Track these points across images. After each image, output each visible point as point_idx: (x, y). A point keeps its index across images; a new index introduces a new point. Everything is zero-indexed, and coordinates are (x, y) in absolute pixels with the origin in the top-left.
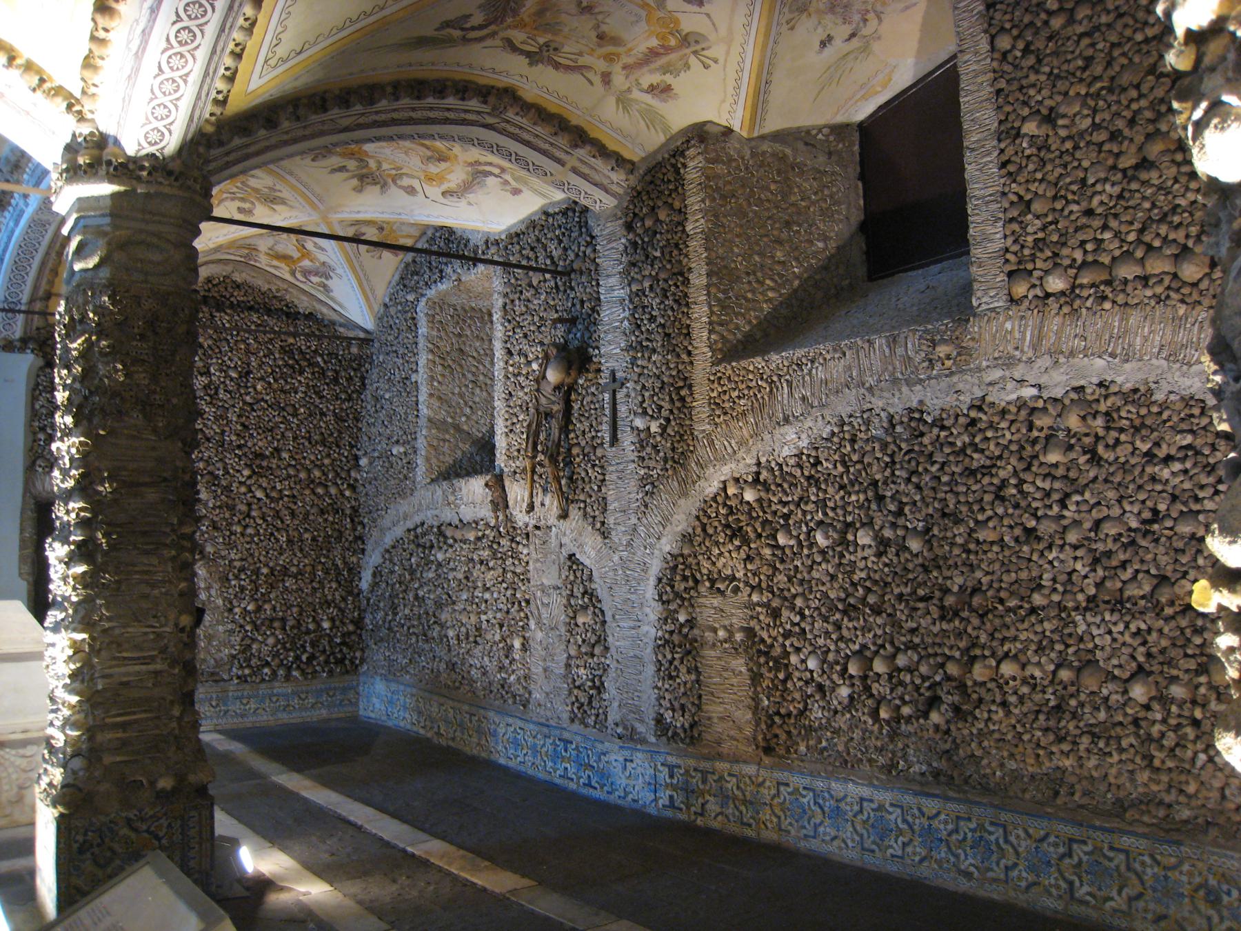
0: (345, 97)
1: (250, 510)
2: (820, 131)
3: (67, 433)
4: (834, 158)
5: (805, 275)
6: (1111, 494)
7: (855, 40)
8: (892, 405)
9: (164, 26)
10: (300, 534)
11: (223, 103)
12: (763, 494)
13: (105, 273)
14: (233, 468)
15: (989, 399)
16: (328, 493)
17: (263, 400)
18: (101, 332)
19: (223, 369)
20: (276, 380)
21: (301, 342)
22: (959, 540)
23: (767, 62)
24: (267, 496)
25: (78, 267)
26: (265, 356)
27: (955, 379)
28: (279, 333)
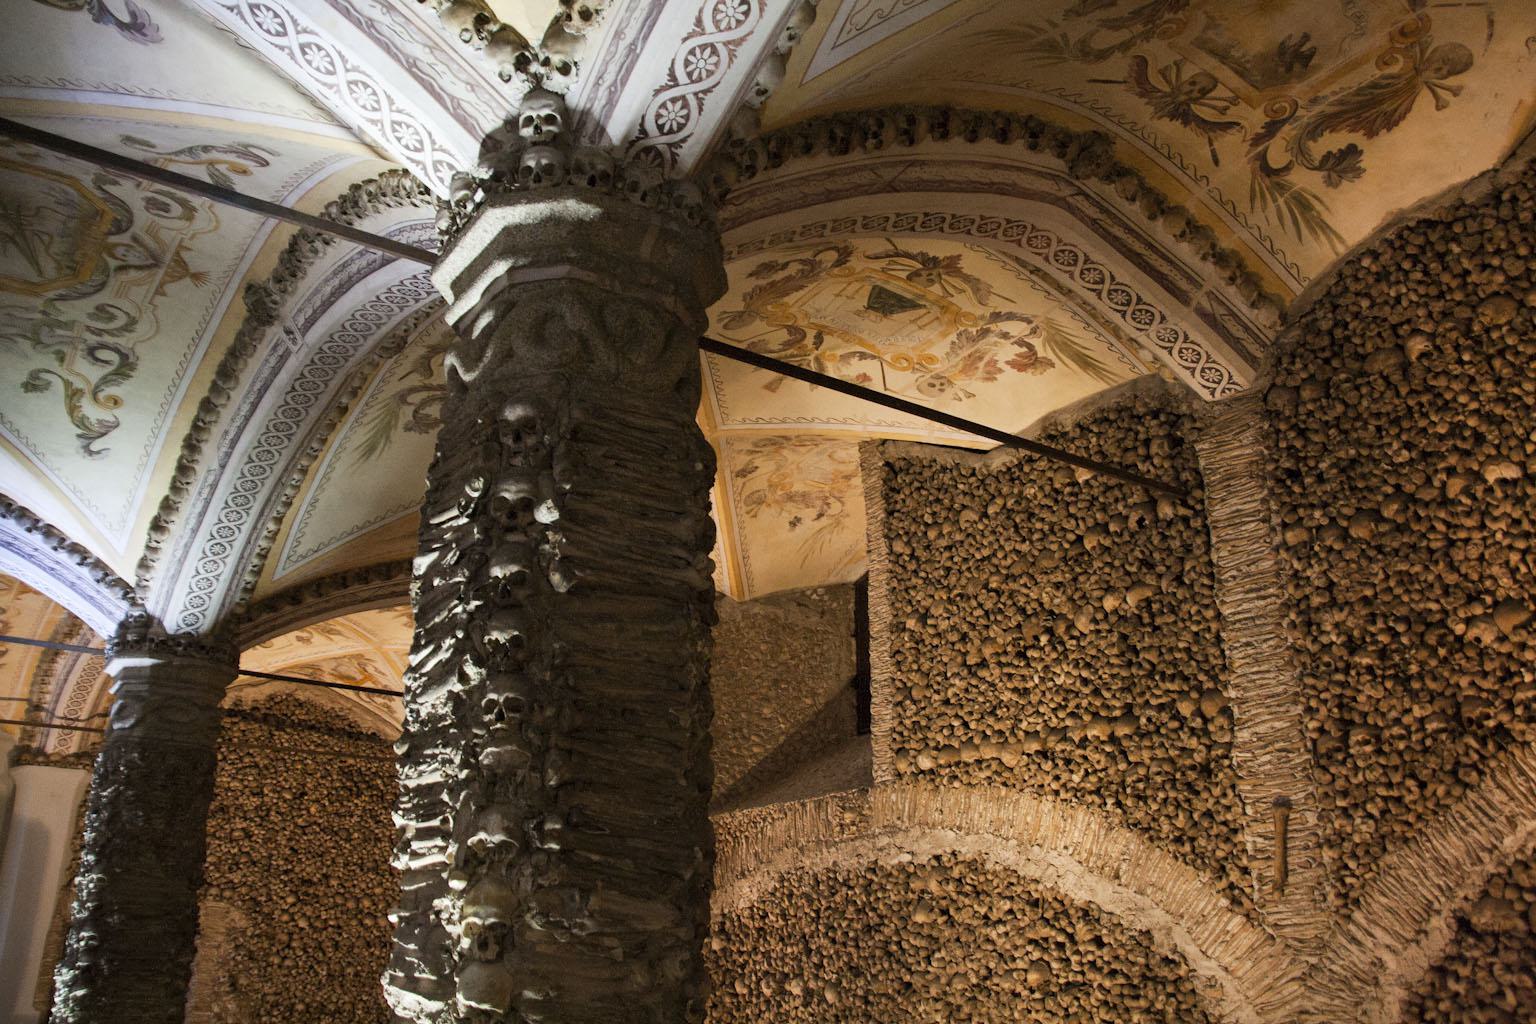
0: (364, 575)
1: (291, 940)
2: (815, 591)
3: (89, 869)
4: (827, 617)
5: (792, 731)
7: (823, 519)
8: (816, 865)
9: (201, 542)
10: (343, 969)
11: (252, 590)
12: (725, 944)
13: (138, 732)
14: (277, 894)
15: (880, 863)
16: (379, 928)
17: (315, 823)
18: (128, 782)
19: (278, 790)
20: (331, 803)
21: (361, 764)
22: (860, 992)
23: (738, 544)
24: (311, 925)
25: (116, 726)
26: (322, 777)
27: (857, 843)
28: (339, 754)
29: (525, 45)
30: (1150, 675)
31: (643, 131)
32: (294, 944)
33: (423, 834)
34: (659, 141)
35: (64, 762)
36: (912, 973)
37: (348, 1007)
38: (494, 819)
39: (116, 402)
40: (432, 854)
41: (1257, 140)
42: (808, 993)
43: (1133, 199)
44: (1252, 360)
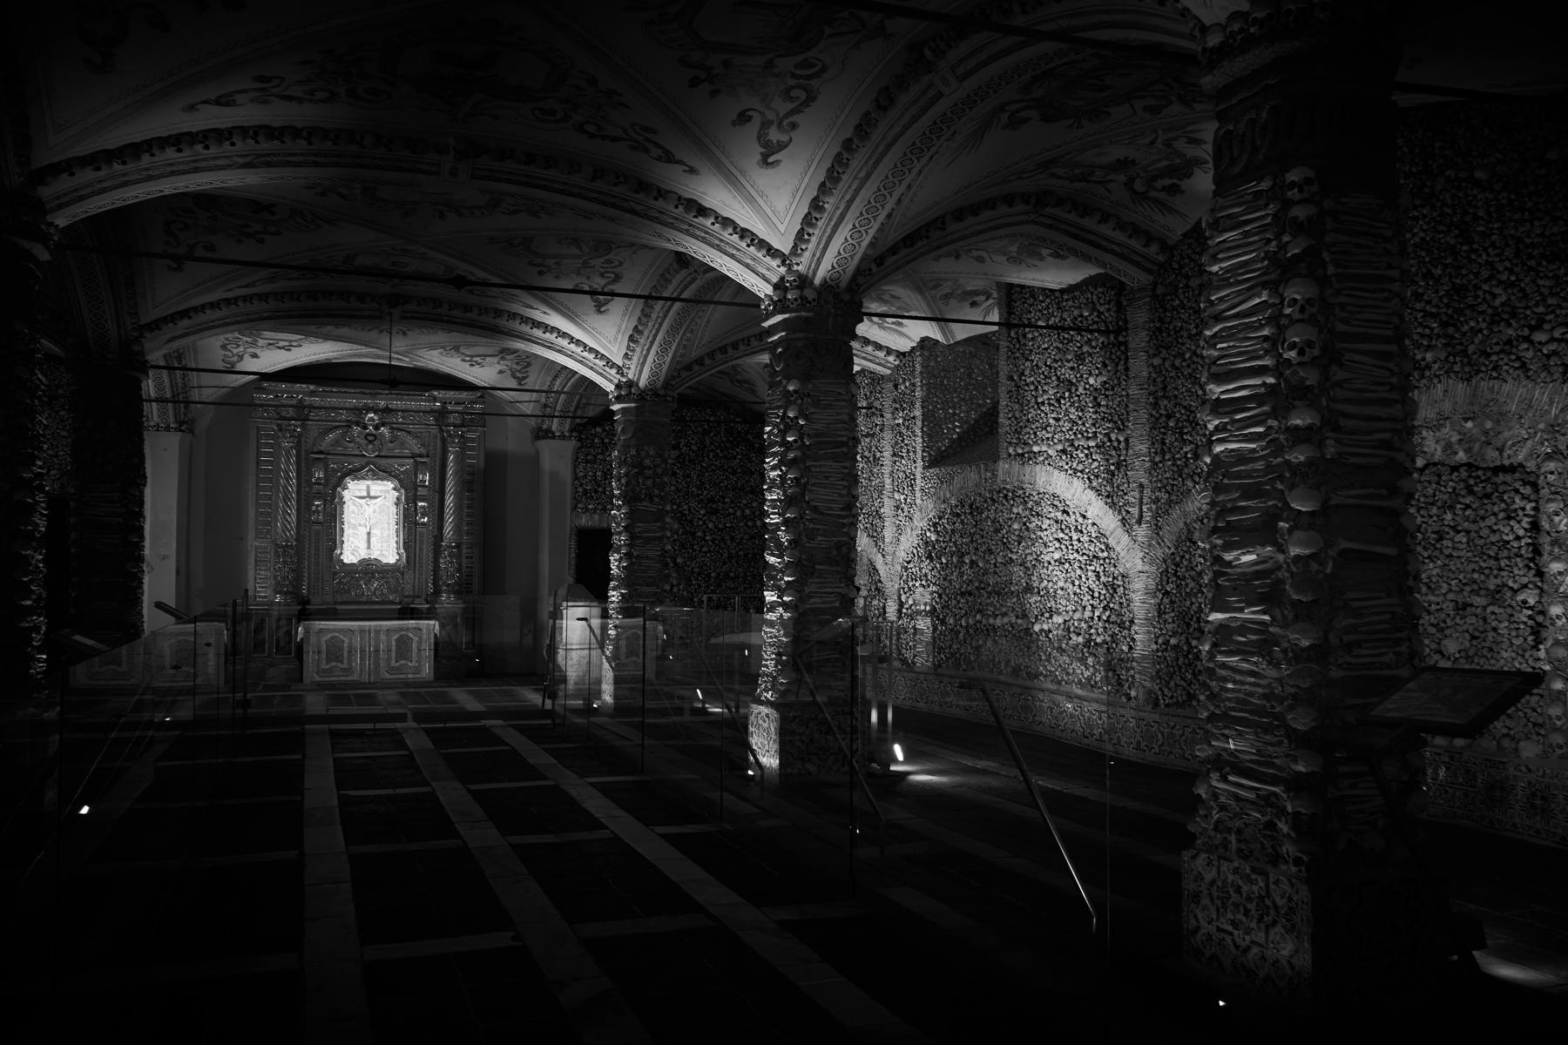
1: (705, 536)
3: (619, 508)
6: (1030, 543)
16: (755, 525)
24: (716, 527)
29: (784, 254)
30: (1103, 419)
31: (826, 282)
32: (707, 538)
33: (774, 513)
34: (832, 283)
35: (563, 437)
36: (1012, 552)
37: (742, 574)
38: (791, 509)
40: (775, 519)
41: (1125, 184)
42: (972, 562)
43: (1070, 212)
44: (1149, 271)
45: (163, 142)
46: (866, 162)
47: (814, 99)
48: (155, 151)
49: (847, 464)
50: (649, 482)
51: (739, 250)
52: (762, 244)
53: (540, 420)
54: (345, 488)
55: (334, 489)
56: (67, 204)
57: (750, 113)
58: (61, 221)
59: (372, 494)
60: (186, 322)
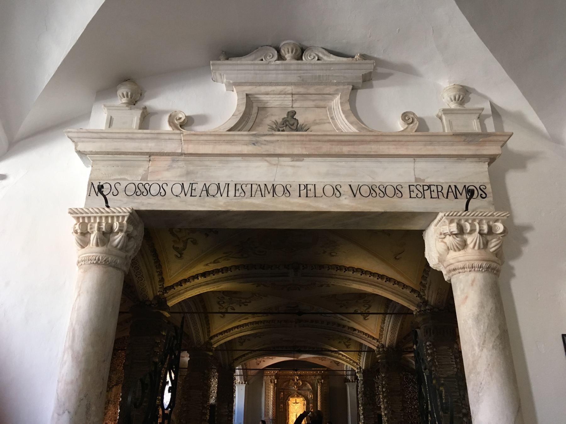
13: (363, 385)
31: (389, 346)
34: (391, 346)
35: (352, 382)
39: (350, 342)
45: (235, 328)
46: (389, 318)
47: (371, 306)
48: (233, 329)
49: (401, 397)
50: (369, 399)
51: (365, 338)
52: (371, 337)
53: (345, 376)
54: (289, 400)
55: (286, 401)
56: (216, 343)
57: (357, 310)
58: (215, 346)
59: (297, 402)
60: (244, 358)
